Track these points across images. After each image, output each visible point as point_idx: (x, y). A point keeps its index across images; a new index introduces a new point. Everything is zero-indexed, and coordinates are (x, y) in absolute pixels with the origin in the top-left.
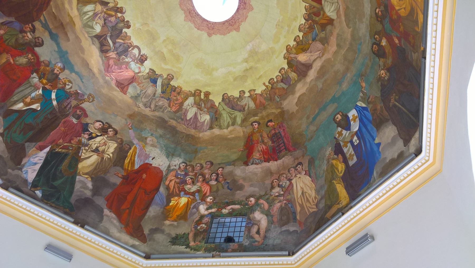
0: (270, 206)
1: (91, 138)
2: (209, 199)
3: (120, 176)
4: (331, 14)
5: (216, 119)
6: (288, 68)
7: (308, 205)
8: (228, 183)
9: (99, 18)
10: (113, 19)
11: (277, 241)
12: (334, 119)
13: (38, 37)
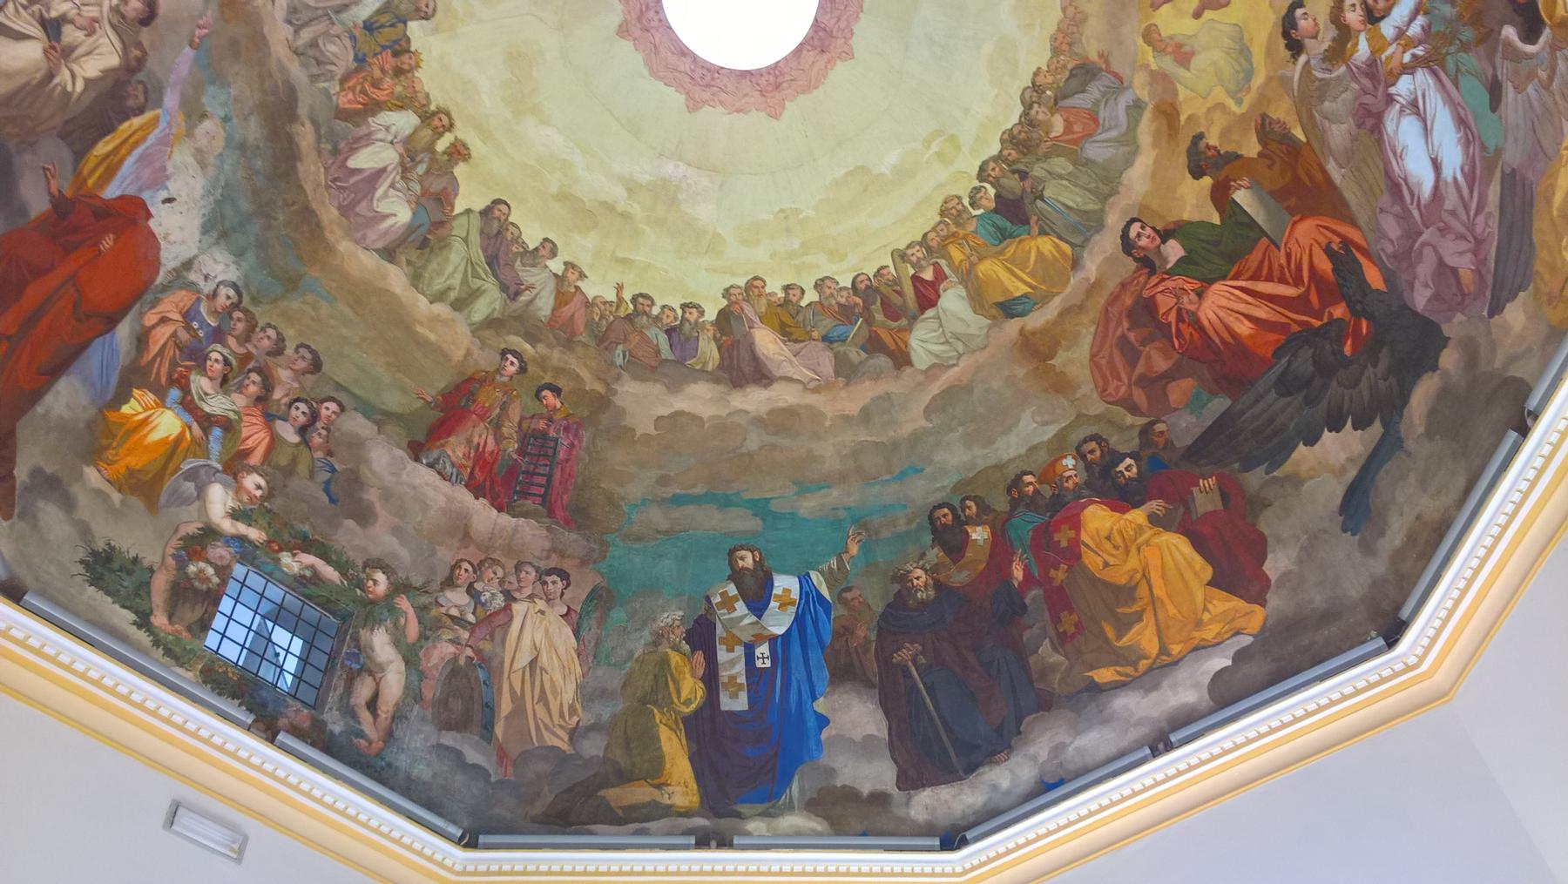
0: (423, 637)
2: (252, 481)
3: (54, 190)
4: (920, 351)
5: (424, 244)
7: (540, 709)
8: (333, 470)
11: (422, 771)
12: (732, 552)
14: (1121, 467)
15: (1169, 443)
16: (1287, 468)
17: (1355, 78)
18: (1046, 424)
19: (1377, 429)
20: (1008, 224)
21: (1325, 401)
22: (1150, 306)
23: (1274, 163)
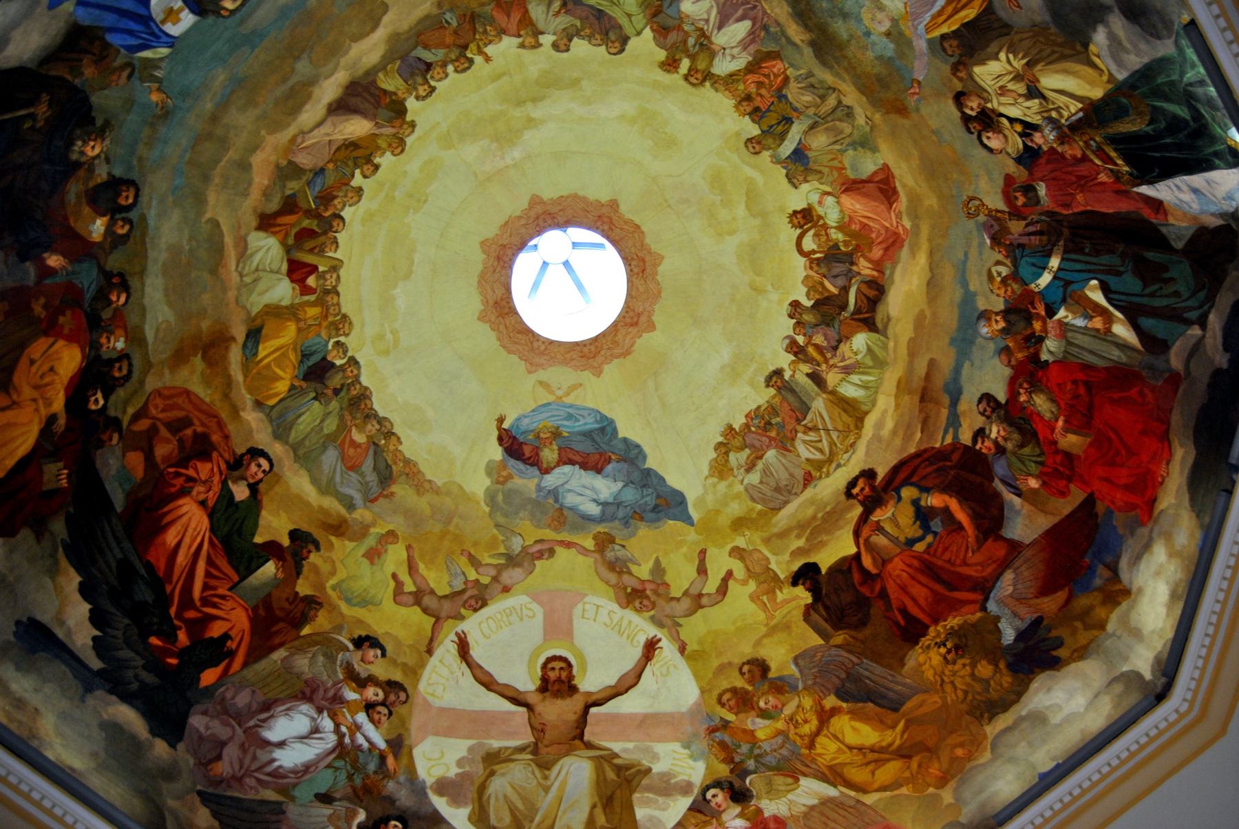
1: (1028, 128)
4: (262, 243)
6: (405, 99)
9: (843, 360)
10: (819, 339)
13: (982, 414)
14: (99, 395)
15: (101, 444)
16: (64, 563)
17: (335, 684)
18: (158, 330)
19: (96, 664)
20: (310, 363)
21: (113, 610)
22: (205, 455)
23: (290, 604)
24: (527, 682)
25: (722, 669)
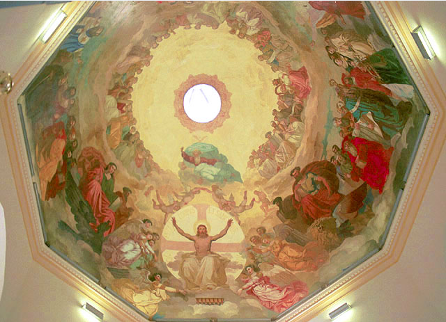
10: (282, 123)
24: (193, 233)
25: (251, 230)
